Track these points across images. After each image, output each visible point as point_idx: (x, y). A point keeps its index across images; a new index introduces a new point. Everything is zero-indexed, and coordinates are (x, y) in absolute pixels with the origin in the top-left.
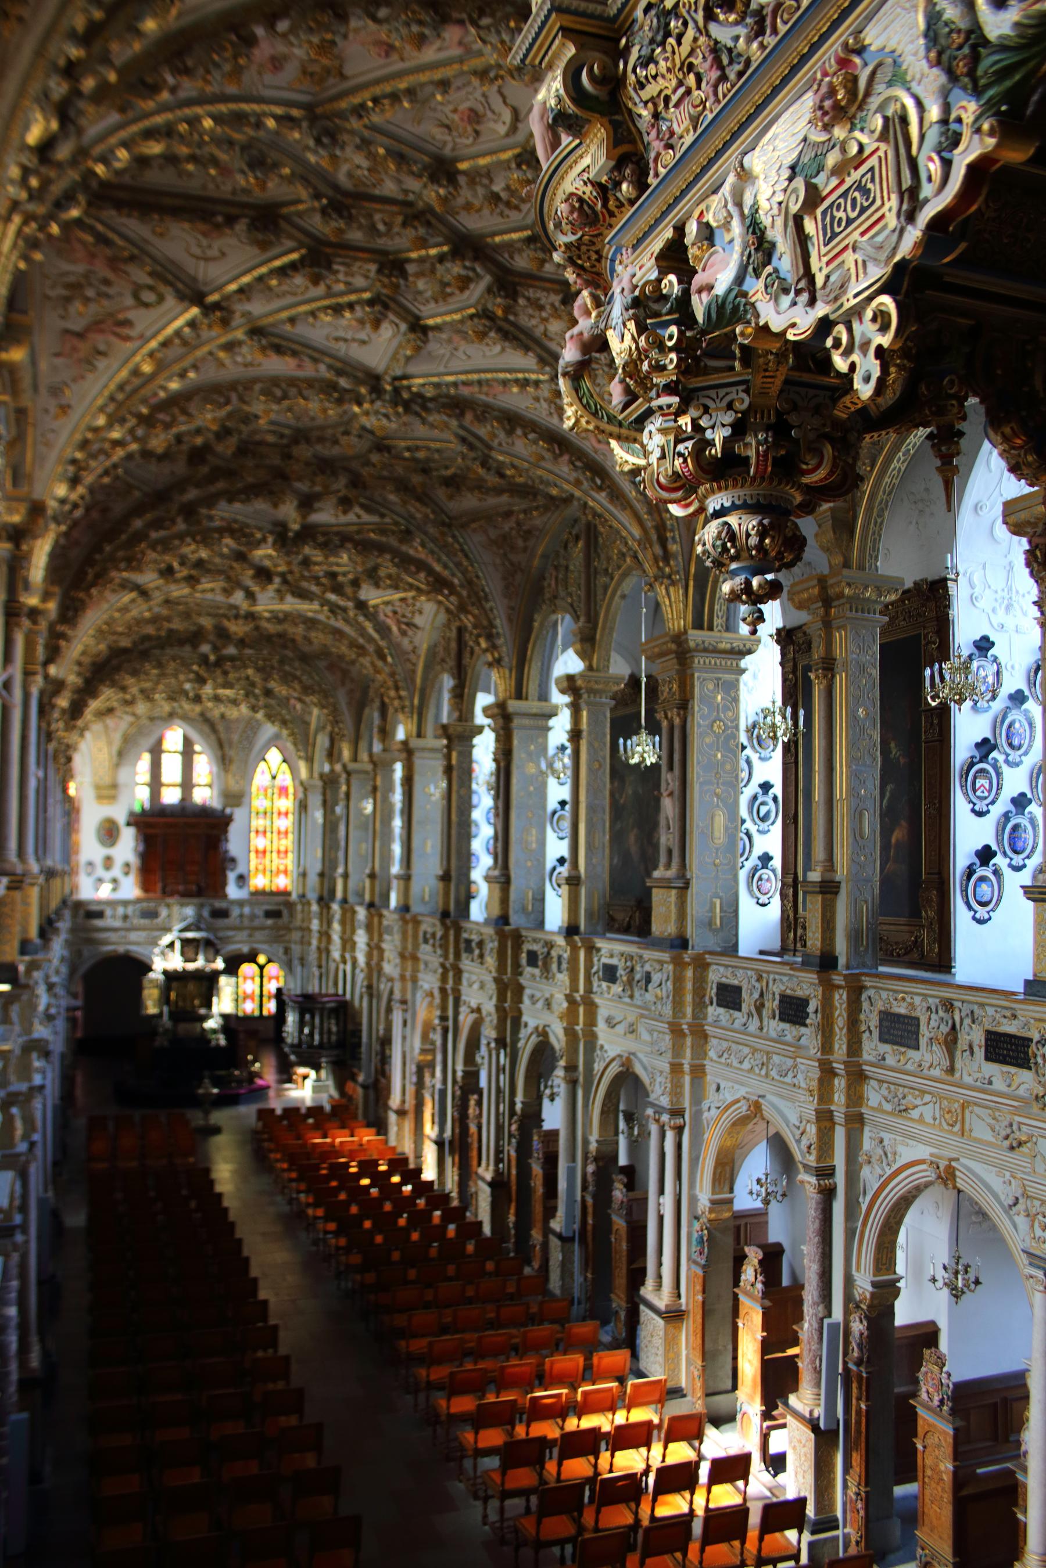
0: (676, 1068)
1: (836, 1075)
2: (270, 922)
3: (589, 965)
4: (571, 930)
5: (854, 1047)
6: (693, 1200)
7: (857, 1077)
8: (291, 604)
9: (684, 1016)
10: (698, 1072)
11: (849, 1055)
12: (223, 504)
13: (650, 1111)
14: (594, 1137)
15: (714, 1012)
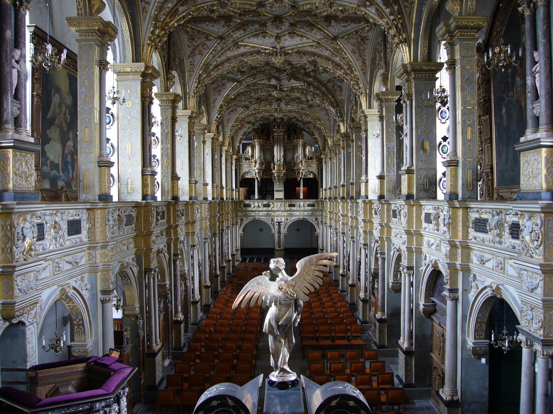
0: (409, 250)
1: (458, 248)
2: (310, 208)
3: (388, 210)
4: (381, 197)
5: (466, 234)
6: (417, 305)
7: (466, 248)
8: (295, 83)
9: (413, 228)
10: (419, 251)
11: (463, 239)
12: (247, 40)
13: (401, 268)
14: (391, 280)
15: (424, 225)
